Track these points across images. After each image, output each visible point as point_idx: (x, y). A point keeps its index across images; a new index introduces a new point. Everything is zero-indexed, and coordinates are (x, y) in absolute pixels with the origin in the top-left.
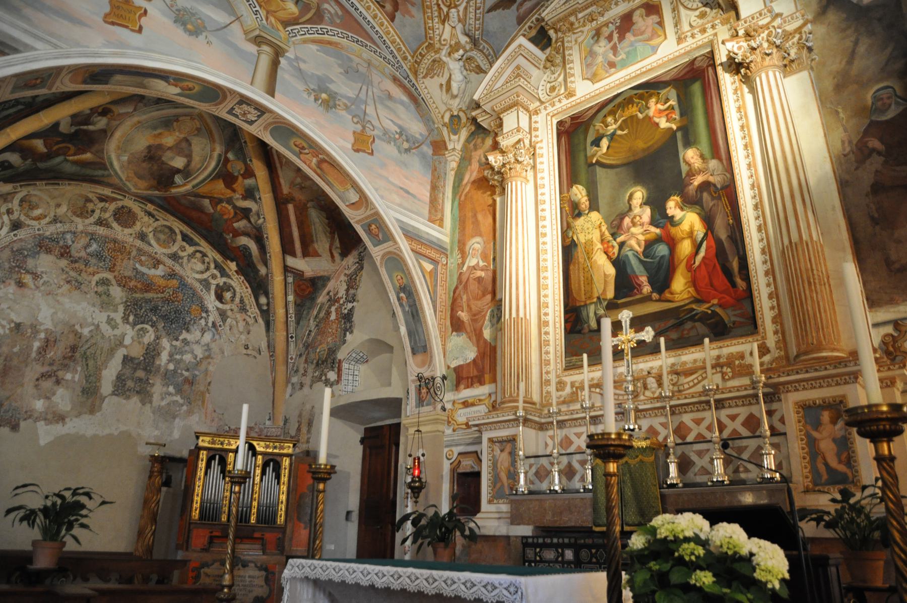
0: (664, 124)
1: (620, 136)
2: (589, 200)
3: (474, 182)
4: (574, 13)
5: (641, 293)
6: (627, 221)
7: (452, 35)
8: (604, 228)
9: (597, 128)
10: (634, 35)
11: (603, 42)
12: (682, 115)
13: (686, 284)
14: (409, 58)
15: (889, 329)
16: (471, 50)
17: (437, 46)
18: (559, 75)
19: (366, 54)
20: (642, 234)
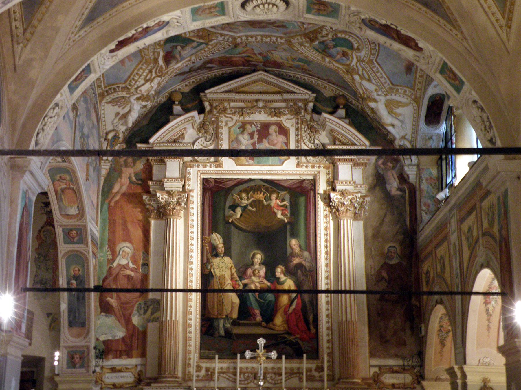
0: (279, 216)
2: (225, 247)
3: (124, 194)
4: (229, 100)
5: (255, 320)
6: (250, 271)
7: (149, 91)
8: (234, 271)
9: (234, 197)
10: (269, 143)
12: (291, 214)
13: (283, 321)
14: (103, 86)
15: (376, 369)
17: (133, 90)
20: (259, 283)
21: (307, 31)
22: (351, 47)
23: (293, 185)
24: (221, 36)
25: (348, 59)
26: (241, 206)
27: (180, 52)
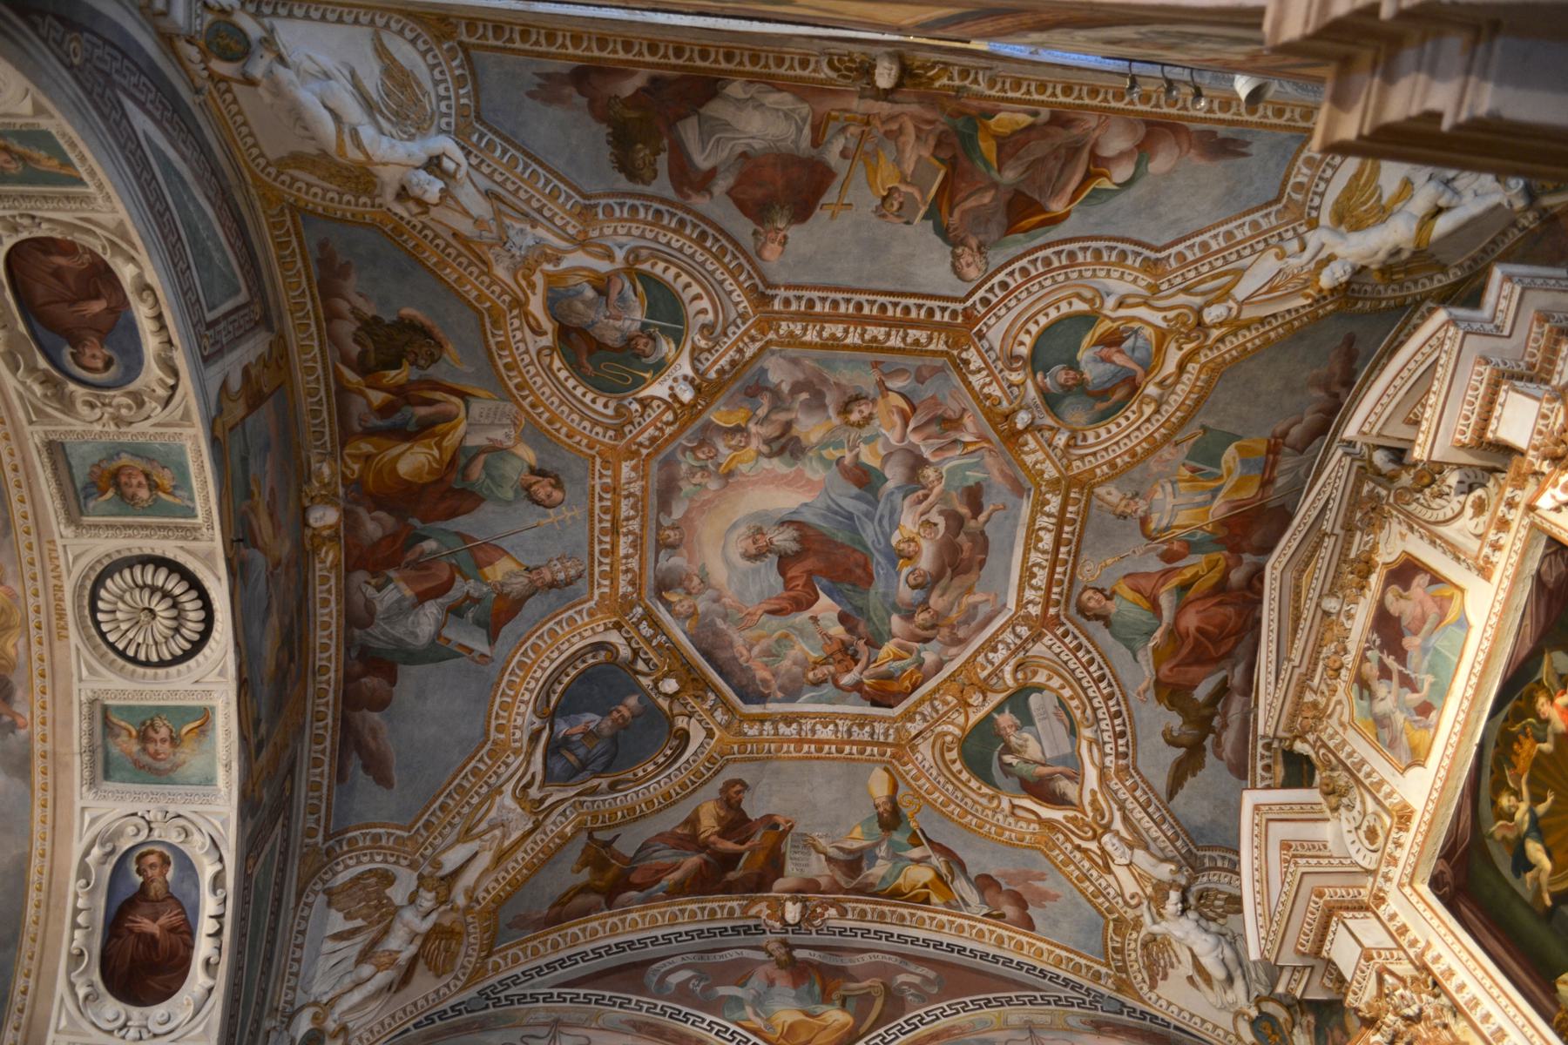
1: (1549, 813)
7: (1139, 878)
9: (1498, 836)
10: (1416, 634)
11: (1381, 689)
14: (1104, 970)
16: (1192, 880)
17: (1130, 914)
18: (1363, 802)
19: (1015, 1015)
21: (994, 437)
22: (1087, 320)
23: (1538, 621)
24: (995, 650)
25: (1136, 332)
26: (1527, 835)
27: (1026, 762)
